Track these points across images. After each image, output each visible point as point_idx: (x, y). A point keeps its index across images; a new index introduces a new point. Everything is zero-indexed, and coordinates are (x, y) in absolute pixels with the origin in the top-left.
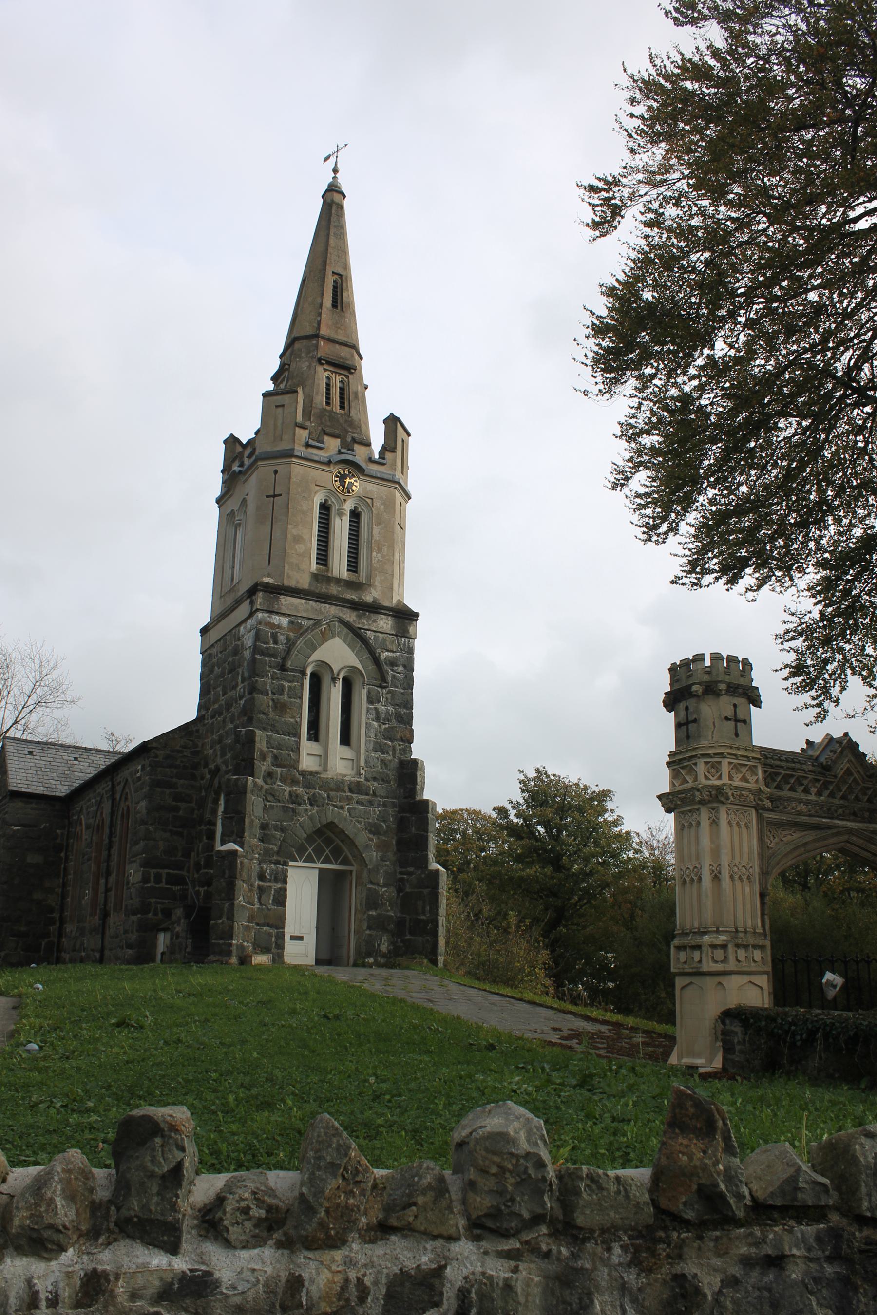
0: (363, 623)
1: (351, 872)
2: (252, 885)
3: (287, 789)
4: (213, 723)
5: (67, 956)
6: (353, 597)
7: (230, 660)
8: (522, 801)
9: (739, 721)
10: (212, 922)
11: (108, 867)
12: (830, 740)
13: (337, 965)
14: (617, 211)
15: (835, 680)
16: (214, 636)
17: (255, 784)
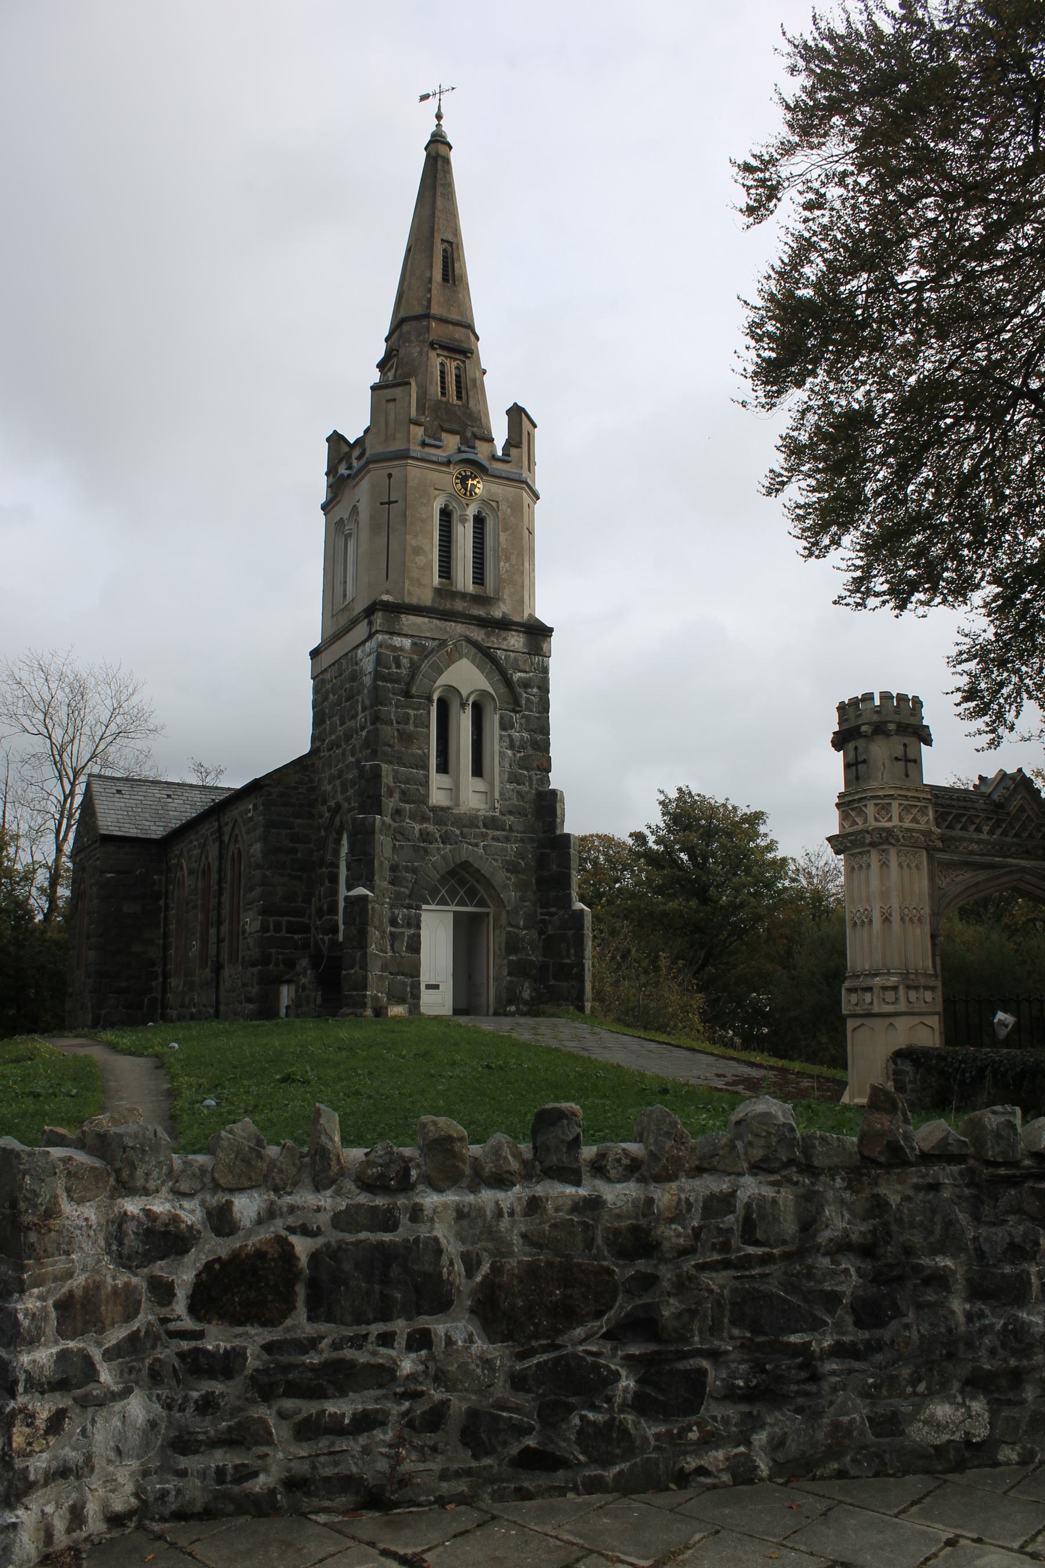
0: (493, 642)
1: (488, 914)
2: (384, 932)
3: (417, 827)
4: (330, 756)
5: (174, 1013)
6: (481, 613)
7: (347, 686)
8: (662, 825)
9: (910, 761)
10: (344, 972)
11: (219, 914)
12: (1003, 776)
13: (477, 1014)
14: (773, 192)
15: (1011, 705)
16: (327, 659)
17: (383, 822)
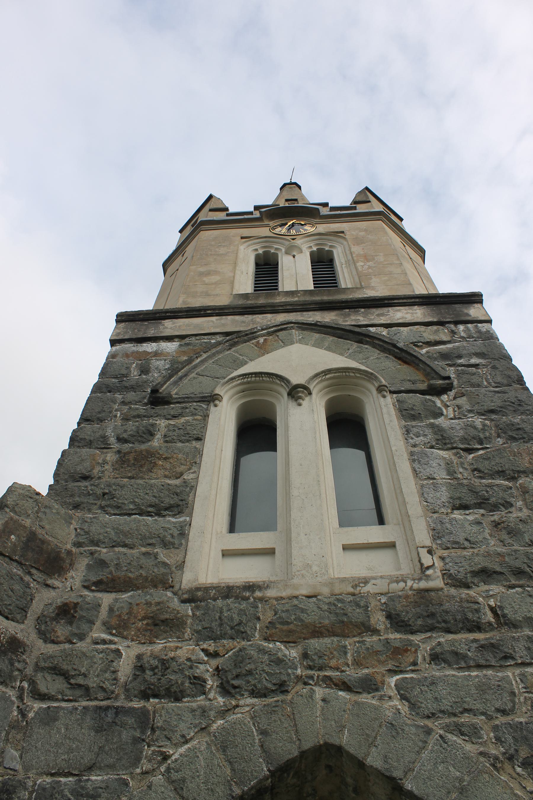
3: (129, 652)
